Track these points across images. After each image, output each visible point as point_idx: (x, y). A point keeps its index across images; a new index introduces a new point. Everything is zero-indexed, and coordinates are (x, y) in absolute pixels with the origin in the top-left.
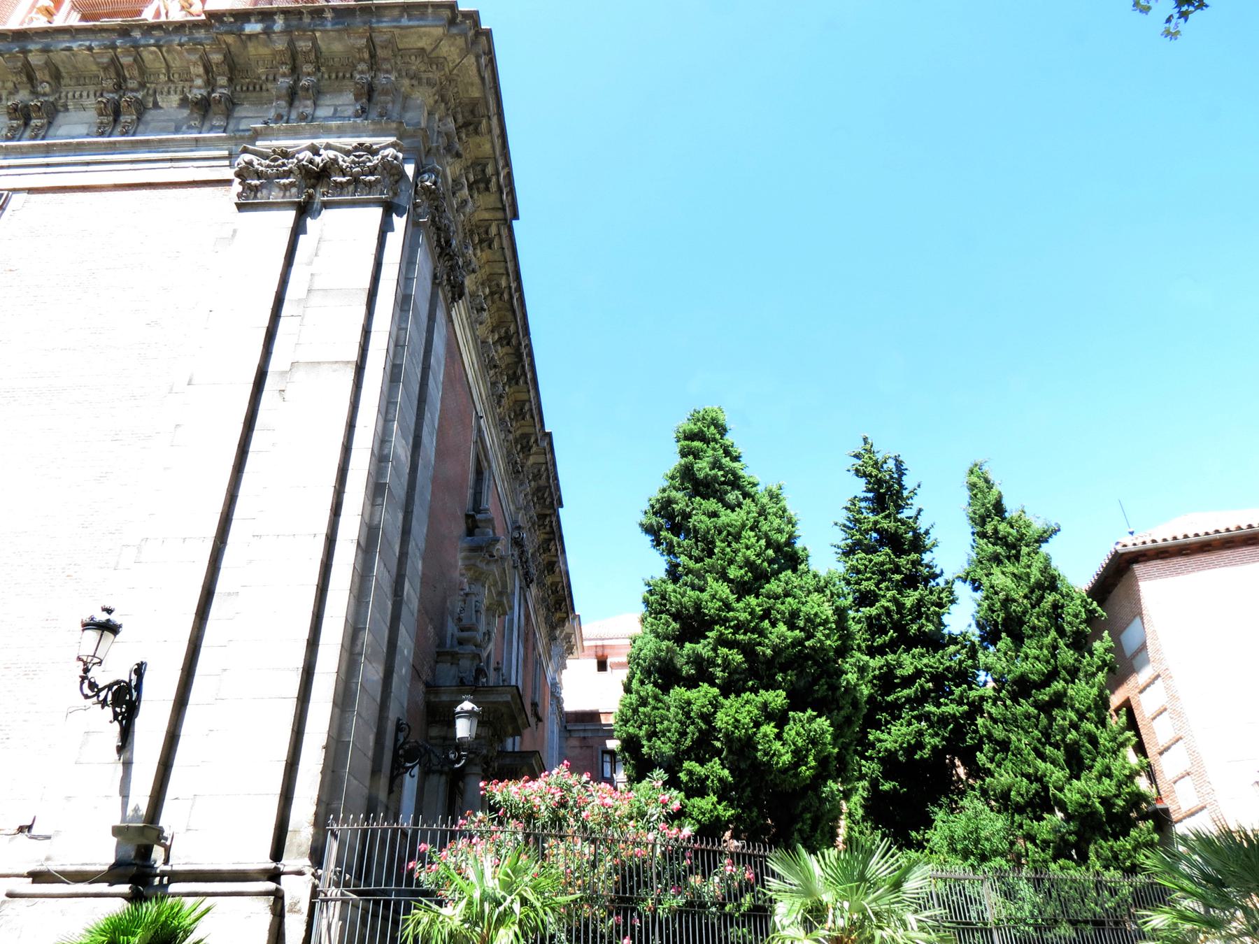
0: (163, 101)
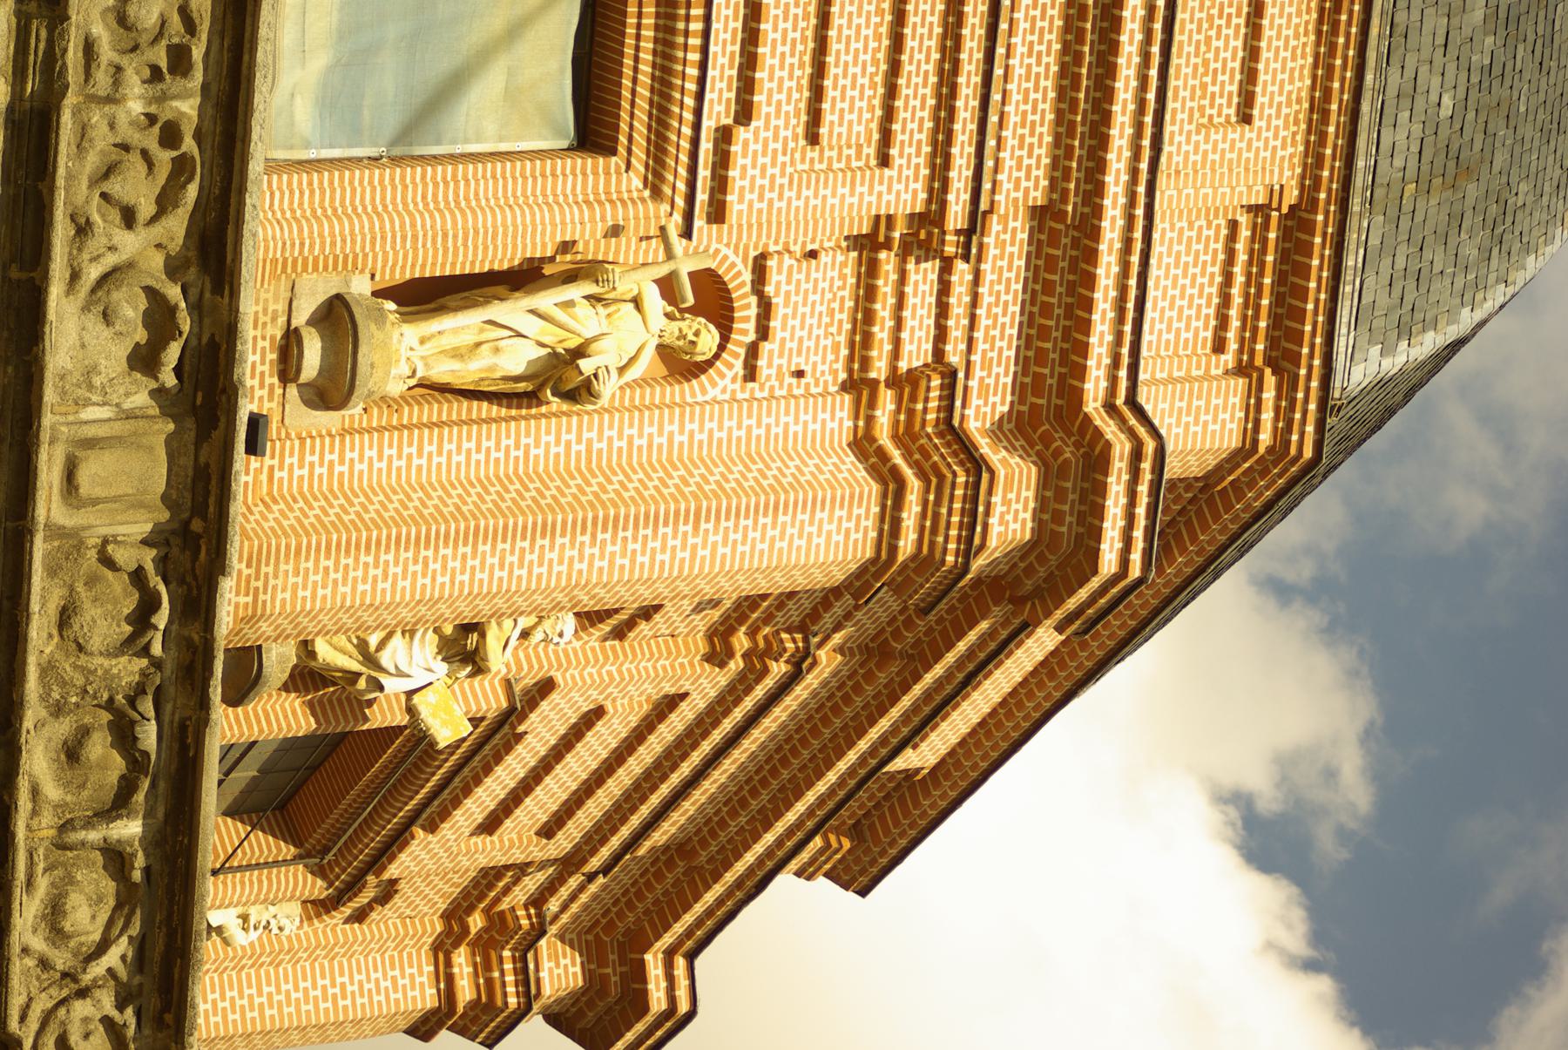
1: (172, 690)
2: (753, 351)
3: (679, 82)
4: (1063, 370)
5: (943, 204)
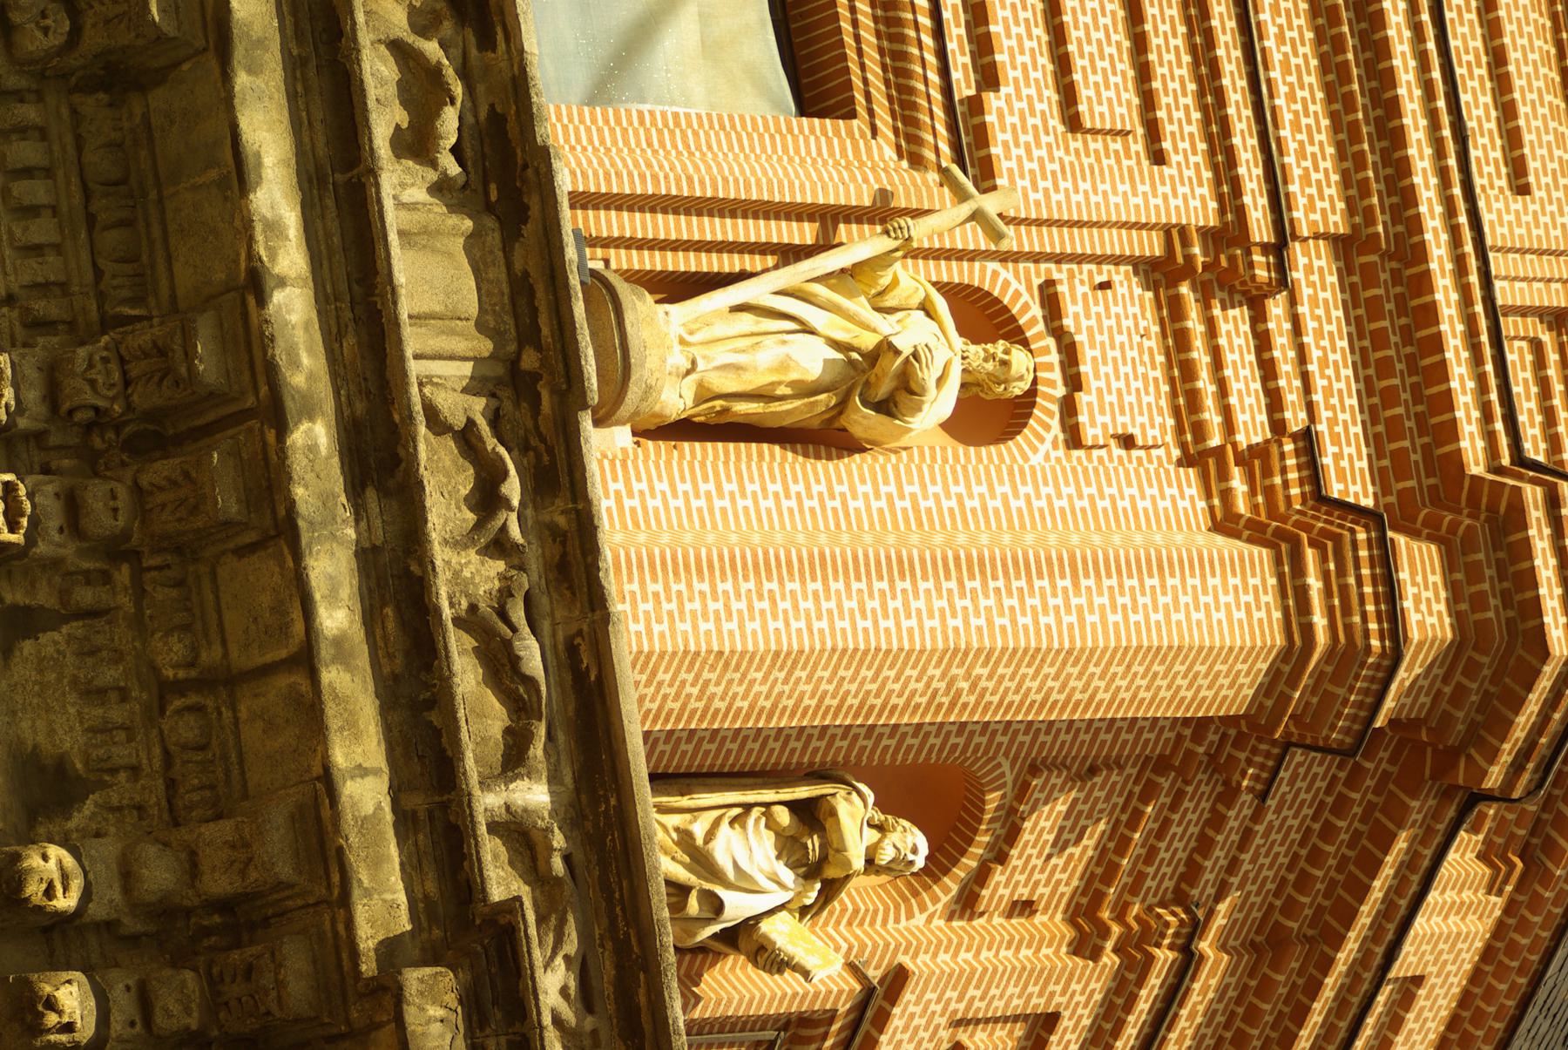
0: (41, 664)
1: (545, 600)
2: (1068, 408)
3: (910, 16)
4: (1426, 440)
5: (1241, 212)
